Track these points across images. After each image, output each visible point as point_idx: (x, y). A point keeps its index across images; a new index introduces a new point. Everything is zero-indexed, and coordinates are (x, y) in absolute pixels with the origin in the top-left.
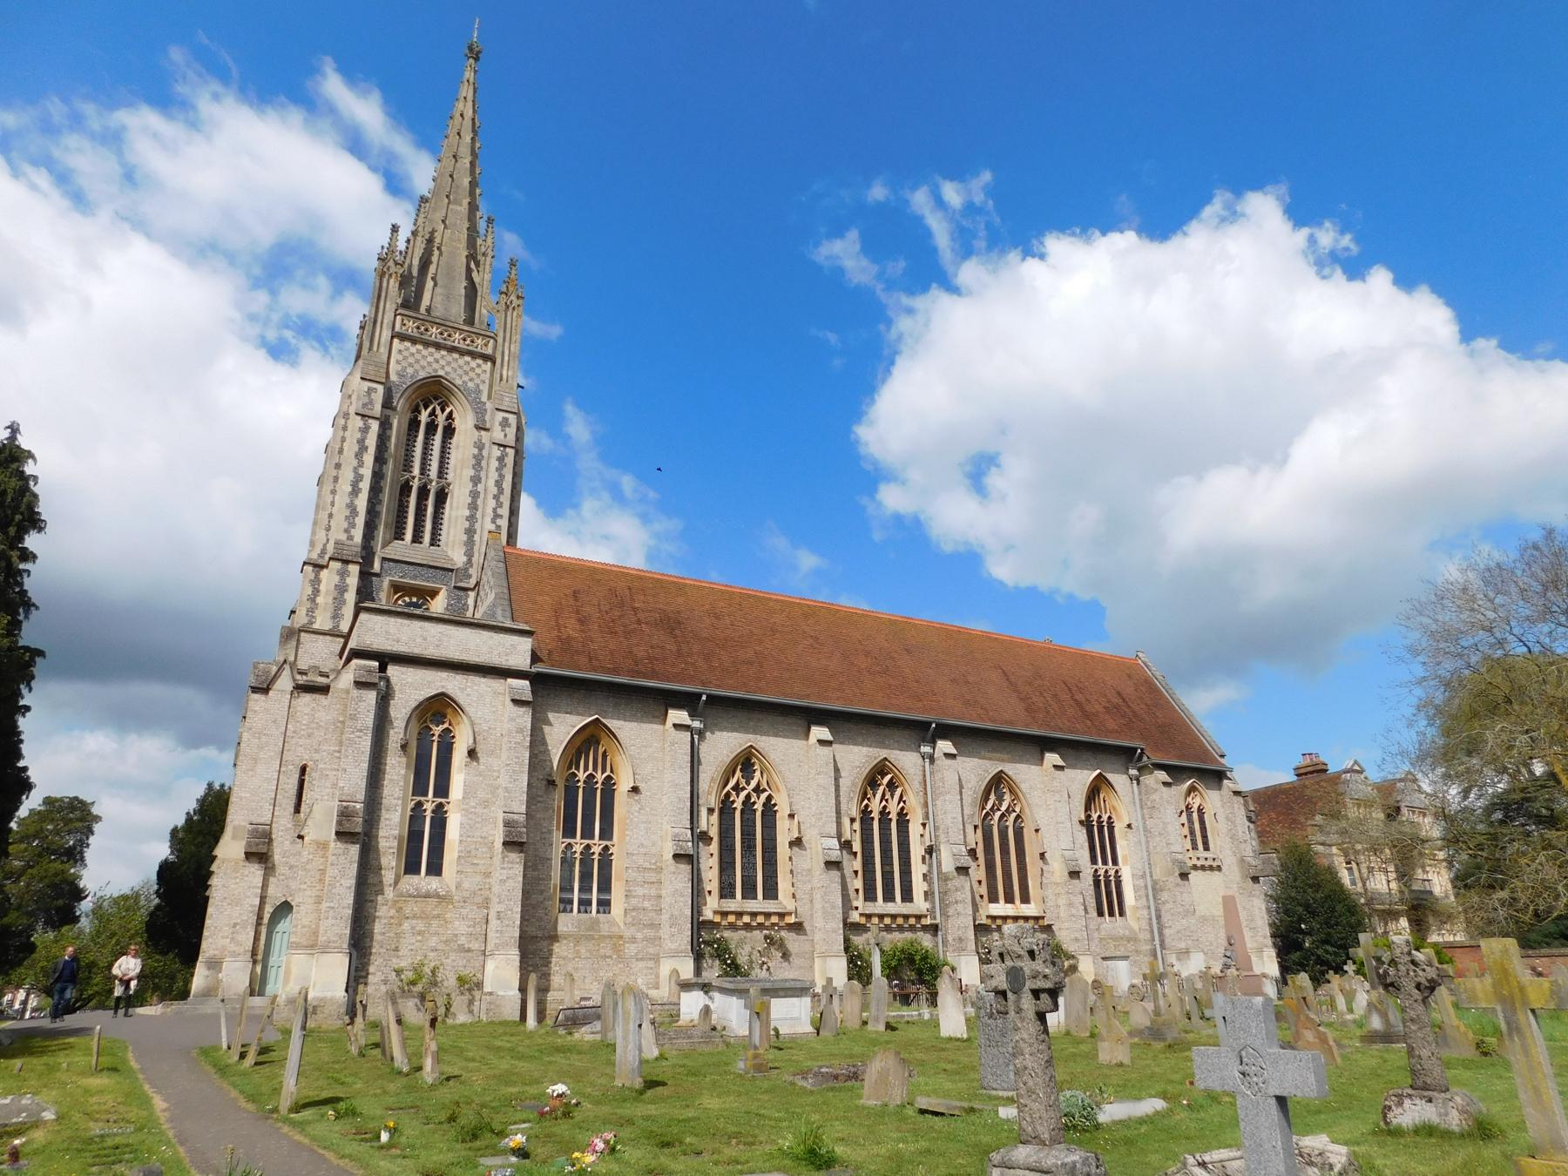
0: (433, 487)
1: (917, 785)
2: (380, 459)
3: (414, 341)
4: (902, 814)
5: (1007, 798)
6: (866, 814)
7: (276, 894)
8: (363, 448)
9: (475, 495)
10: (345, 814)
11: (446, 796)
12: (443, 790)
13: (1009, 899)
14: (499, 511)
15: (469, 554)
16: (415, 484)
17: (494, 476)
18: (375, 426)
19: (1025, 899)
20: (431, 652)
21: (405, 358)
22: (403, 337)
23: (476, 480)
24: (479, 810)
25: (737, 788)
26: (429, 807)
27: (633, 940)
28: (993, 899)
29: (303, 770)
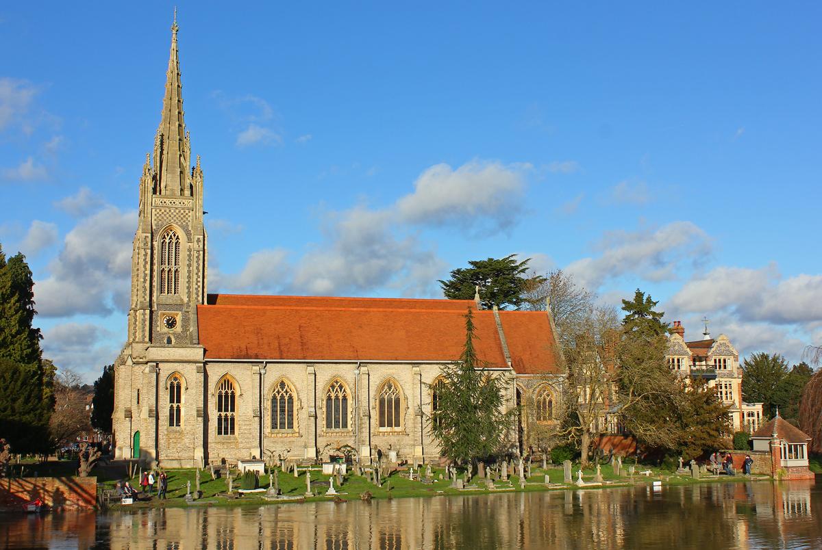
0: (173, 270)
1: (351, 385)
5: (393, 387)
6: (329, 398)
7: (135, 429)
9: (189, 272)
10: (150, 411)
11: (180, 402)
12: (179, 401)
13: (390, 425)
14: (199, 279)
16: (167, 270)
17: (195, 265)
19: (398, 425)
20: (171, 358)
21: (158, 217)
23: (189, 266)
24: (190, 406)
25: (278, 392)
26: (175, 405)
27: (242, 442)
28: (382, 425)
29: (139, 390)
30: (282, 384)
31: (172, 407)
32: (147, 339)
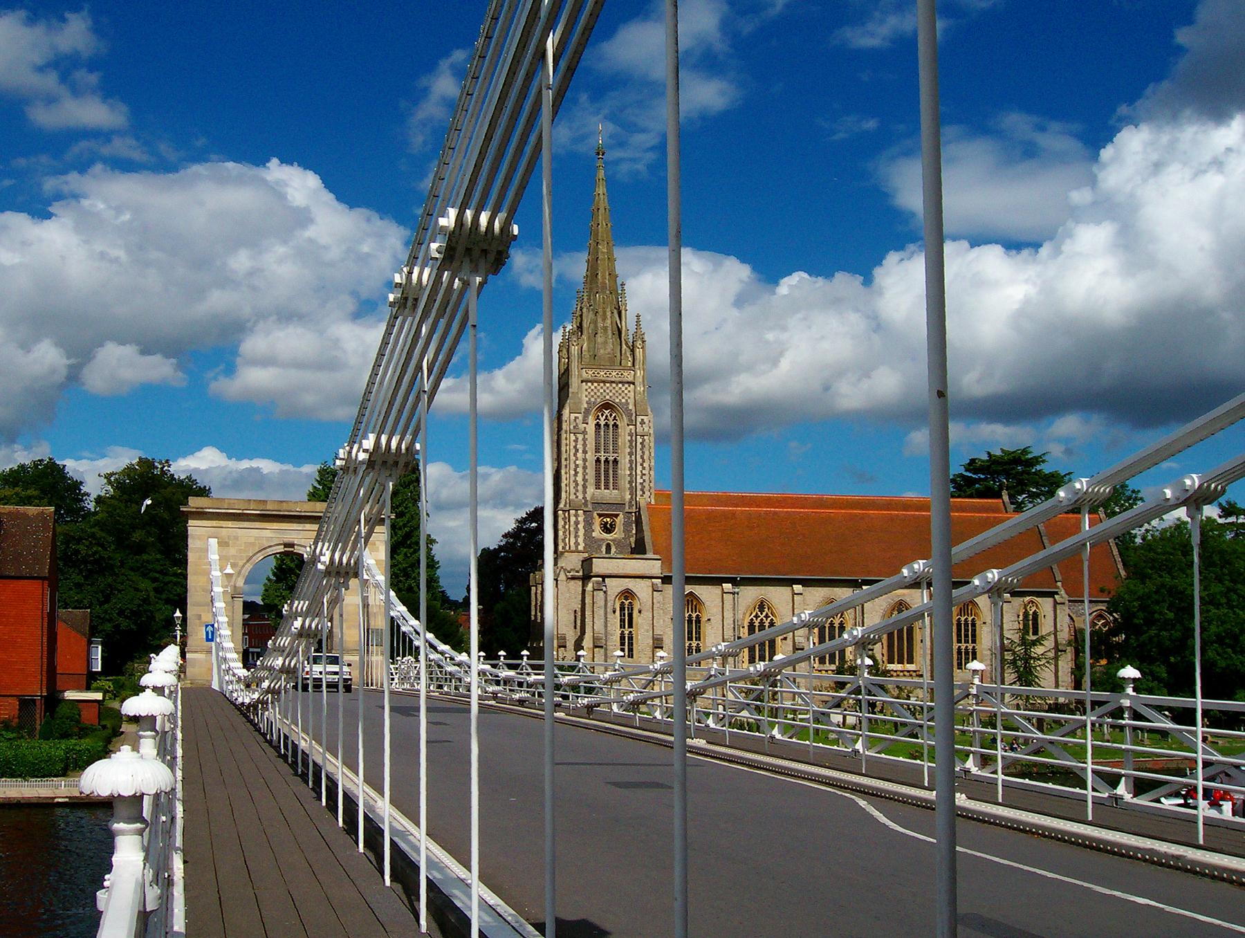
0: (611, 459)
2: (585, 452)
3: (592, 382)
4: (841, 624)
8: (577, 451)
9: (631, 462)
12: (630, 626)
15: (633, 491)
16: (603, 459)
18: (580, 437)
19: (910, 661)
20: (621, 572)
22: (587, 381)
23: (630, 454)
25: (757, 616)
26: (627, 632)
28: (891, 661)
30: (761, 608)
31: (622, 633)
32: (581, 548)
